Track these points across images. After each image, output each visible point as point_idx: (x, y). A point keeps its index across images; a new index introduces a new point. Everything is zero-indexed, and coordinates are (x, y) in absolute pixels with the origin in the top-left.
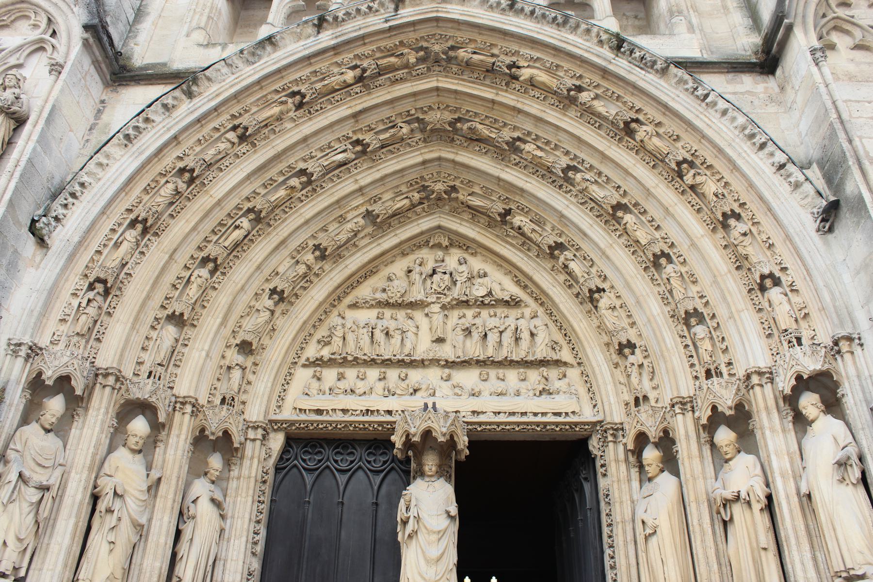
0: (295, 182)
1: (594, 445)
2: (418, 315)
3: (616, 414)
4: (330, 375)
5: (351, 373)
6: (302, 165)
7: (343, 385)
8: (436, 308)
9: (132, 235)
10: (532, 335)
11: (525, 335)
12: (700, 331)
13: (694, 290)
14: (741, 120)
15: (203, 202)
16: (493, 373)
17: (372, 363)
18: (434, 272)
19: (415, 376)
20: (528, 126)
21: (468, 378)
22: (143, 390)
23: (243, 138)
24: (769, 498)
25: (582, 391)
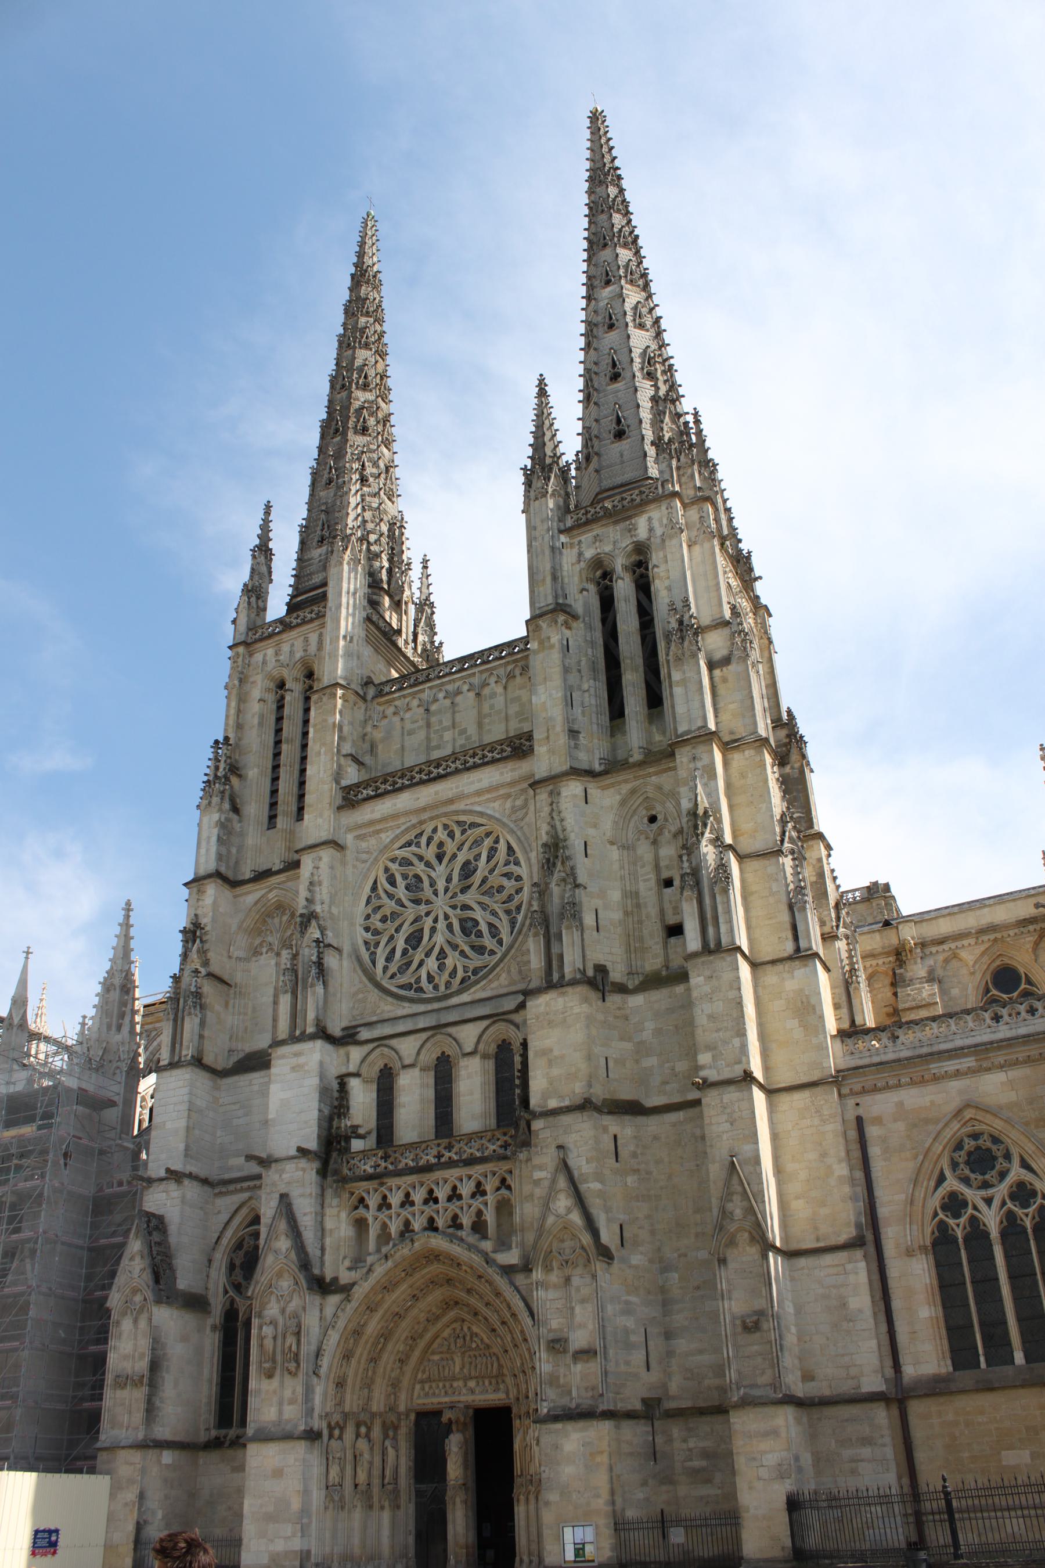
0: (397, 1318)
6: (397, 1310)
11: (489, 1366)
15: (365, 1338)
21: (472, 1384)
22: (362, 1417)
23: (372, 1311)
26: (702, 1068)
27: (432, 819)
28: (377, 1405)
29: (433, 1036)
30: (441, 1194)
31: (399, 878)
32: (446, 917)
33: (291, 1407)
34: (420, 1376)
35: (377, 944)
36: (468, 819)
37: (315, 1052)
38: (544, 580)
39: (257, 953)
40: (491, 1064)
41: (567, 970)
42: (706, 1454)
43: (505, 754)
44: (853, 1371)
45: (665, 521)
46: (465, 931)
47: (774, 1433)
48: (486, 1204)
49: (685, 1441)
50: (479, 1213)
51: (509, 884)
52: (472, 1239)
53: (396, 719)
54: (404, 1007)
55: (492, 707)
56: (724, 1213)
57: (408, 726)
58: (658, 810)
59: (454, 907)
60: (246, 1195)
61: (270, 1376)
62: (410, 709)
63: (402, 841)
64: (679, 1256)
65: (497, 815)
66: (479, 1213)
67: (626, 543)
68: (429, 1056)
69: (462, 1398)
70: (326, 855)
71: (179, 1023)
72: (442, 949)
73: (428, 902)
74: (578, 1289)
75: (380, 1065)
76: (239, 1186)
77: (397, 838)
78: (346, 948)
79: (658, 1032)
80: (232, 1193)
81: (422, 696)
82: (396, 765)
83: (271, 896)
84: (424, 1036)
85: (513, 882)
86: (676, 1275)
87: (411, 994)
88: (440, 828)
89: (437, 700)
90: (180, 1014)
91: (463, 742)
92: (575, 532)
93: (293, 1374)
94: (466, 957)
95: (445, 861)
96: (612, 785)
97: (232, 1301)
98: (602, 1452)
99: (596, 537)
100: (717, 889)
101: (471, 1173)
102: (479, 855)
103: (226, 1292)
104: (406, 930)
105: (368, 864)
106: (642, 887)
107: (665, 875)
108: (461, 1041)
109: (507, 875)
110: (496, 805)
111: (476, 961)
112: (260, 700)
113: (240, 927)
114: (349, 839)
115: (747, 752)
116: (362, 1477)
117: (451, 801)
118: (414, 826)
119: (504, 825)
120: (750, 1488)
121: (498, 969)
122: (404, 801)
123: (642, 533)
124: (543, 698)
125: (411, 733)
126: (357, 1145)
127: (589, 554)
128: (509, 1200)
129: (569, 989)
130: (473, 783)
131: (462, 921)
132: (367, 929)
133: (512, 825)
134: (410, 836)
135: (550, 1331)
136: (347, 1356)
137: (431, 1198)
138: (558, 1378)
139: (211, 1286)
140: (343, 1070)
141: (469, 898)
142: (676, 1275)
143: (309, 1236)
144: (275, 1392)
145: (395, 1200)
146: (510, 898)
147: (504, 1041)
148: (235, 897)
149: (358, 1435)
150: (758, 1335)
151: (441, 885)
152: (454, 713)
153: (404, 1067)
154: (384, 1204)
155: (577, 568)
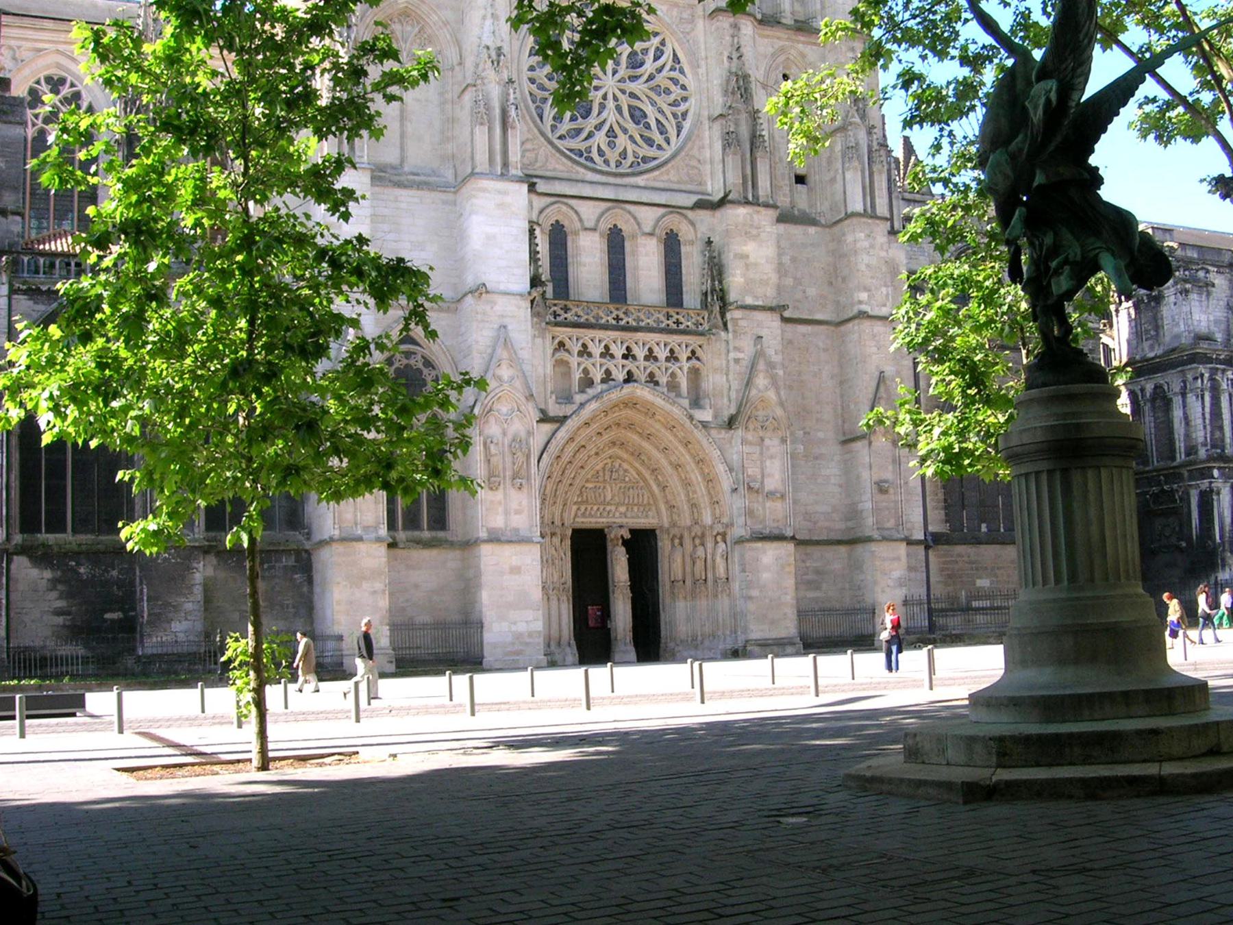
1: (658, 532)
3: (666, 525)
19: (608, 508)
20: (654, 431)
26: (860, 302)
32: (615, 98)
33: (517, 516)
42: (818, 572)
46: (632, 116)
47: (898, 559)
51: (676, 92)
59: (623, 92)
64: (805, 433)
66: (673, 375)
68: (605, 225)
69: (616, 520)
72: (611, 127)
74: (768, 448)
87: (582, 160)
94: (635, 143)
96: (768, 36)
102: (647, 50)
109: (675, 81)
131: (629, 106)
132: (532, 81)
144: (500, 503)
146: (675, 104)
153: (586, 229)
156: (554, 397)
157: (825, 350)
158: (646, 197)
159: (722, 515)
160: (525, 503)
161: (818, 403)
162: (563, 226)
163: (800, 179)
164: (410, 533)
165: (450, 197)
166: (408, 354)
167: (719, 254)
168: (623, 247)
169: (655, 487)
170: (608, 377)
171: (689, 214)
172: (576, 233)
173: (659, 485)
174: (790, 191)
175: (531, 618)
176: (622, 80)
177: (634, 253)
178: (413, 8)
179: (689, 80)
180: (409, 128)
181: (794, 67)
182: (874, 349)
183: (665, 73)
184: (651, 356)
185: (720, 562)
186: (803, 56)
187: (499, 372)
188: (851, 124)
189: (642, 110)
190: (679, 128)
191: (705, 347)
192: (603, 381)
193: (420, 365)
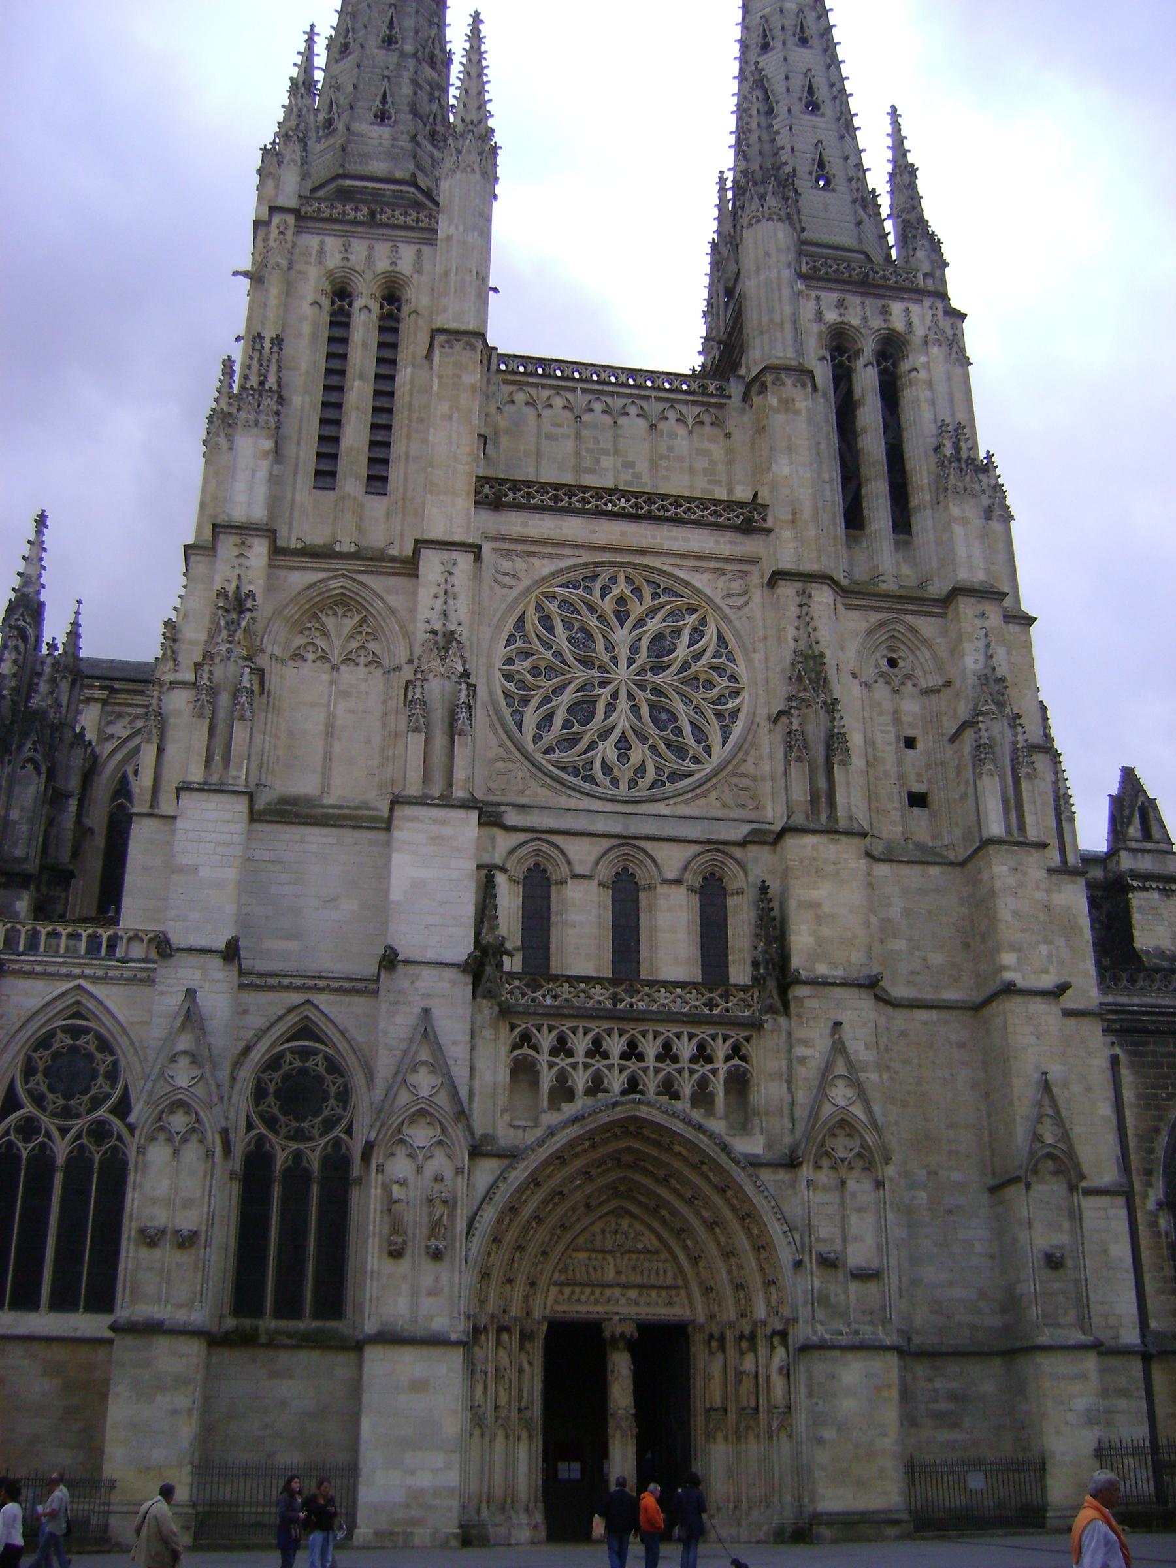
1: (690, 1329)
2: (609, 1257)
3: (701, 1318)
4: (567, 1291)
5: (578, 1290)
7: (575, 1297)
8: (618, 1255)
9: (494, 1247)
10: (665, 1271)
11: (661, 1272)
12: (742, 1294)
13: (742, 1273)
14: (773, 1203)
16: (645, 1291)
17: (587, 1285)
18: (616, 1232)
19: (608, 1292)
21: (633, 1294)
22: (506, 1321)
24: (757, 1373)
25: (686, 1302)
27: (612, 564)
28: (515, 1310)
29: (619, 846)
30: (651, 1048)
31: (559, 626)
34: (556, 1276)
35: (525, 701)
36: (663, 582)
37: (466, 825)
38: (782, 323)
39: (297, 656)
40: (695, 899)
41: (841, 812)
42: (953, 1397)
43: (721, 520)
44: (1112, 1321)
45: (928, 323)
46: (655, 720)
47: (1084, 1376)
48: (714, 1072)
49: (930, 1380)
50: (703, 1083)
52: (697, 1115)
53: (530, 412)
54: (569, 796)
55: (671, 449)
56: (1037, 1137)
57: (547, 427)
58: (903, 652)
59: (642, 687)
60: (297, 998)
61: (396, 1254)
62: (551, 406)
63: (566, 578)
64: (929, 1173)
65: (708, 591)
66: (703, 1083)
67: (876, 323)
68: (606, 871)
69: (621, 1310)
70: (464, 561)
71: (221, 727)
73: (602, 669)
74: (854, 1194)
75: (531, 862)
76: (286, 981)
77: (560, 572)
78: (482, 692)
79: (907, 913)
80: (271, 988)
81: (570, 396)
82: (528, 472)
83: (333, 584)
84: (606, 843)
85: (725, 682)
86: (924, 1195)
88: (622, 578)
89: (592, 410)
90: (222, 715)
91: (629, 477)
92: (813, 283)
93: (436, 1255)
94: (660, 756)
95: (629, 623)
97: (261, 1139)
98: (889, 1386)
99: (841, 304)
100: (1022, 772)
101: (661, 1029)
102: (678, 632)
103: (250, 1126)
104: (568, 697)
105: (515, 593)
106: (879, 738)
107: (910, 733)
108: (659, 861)
110: (706, 577)
111: (674, 763)
112: (316, 303)
113: (278, 612)
114: (487, 548)
115: (1011, 626)
116: (503, 1400)
117: (643, 552)
118: (586, 564)
119: (717, 608)
120: (1058, 1433)
121: (709, 784)
122: (573, 528)
123: (899, 325)
124: (786, 471)
125: (549, 437)
126: (508, 964)
127: (831, 316)
128: (746, 1072)
129: (844, 839)
130: (676, 539)
131: (652, 707)
132: (508, 677)
133: (728, 611)
134: (580, 574)
135: (818, 1240)
136: (496, 1240)
137: (632, 1052)
138: (828, 1297)
139: (232, 1115)
140: (486, 859)
141: (663, 679)
142: (924, 1195)
143: (460, 1073)
144: (405, 1277)
145: (580, 1044)
146: (720, 699)
147: (712, 874)
148: (271, 566)
149: (499, 1343)
150: (1062, 1271)
151: (623, 653)
152: (616, 437)
153: (576, 876)
154: (561, 1047)
155: (815, 328)
156: (507, 1117)
157: (961, 1045)
158: (670, 830)
159: (781, 1302)
160: (444, 1278)
161: (951, 1125)
162: (545, 871)
163: (918, 800)
164: (283, 1324)
165: (381, 836)
166: (305, 1054)
167: (782, 904)
168: (637, 900)
169: (683, 1258)
170: (597, 1086)
171: (737, 852)
172: (563, 882)
173: (688, 1256)
174: (902, 816)
175: (441, 1465)
176: (642, 671)
177: (650, 908)
178: (351, 595)
179: (741, 669)
180: (337, 748)
181: (903, 647)
182: (1032, 1039)
183: (704, 660)
184: (667, 1053)
185: (778, 1384)
186: (914, 630)
187: (413, 1079)
188: (981, 713)
189: (668, 711)
190: (726, 732)
191: (754, 1041)
192: (590, 1092)
193: (321, 1069)
